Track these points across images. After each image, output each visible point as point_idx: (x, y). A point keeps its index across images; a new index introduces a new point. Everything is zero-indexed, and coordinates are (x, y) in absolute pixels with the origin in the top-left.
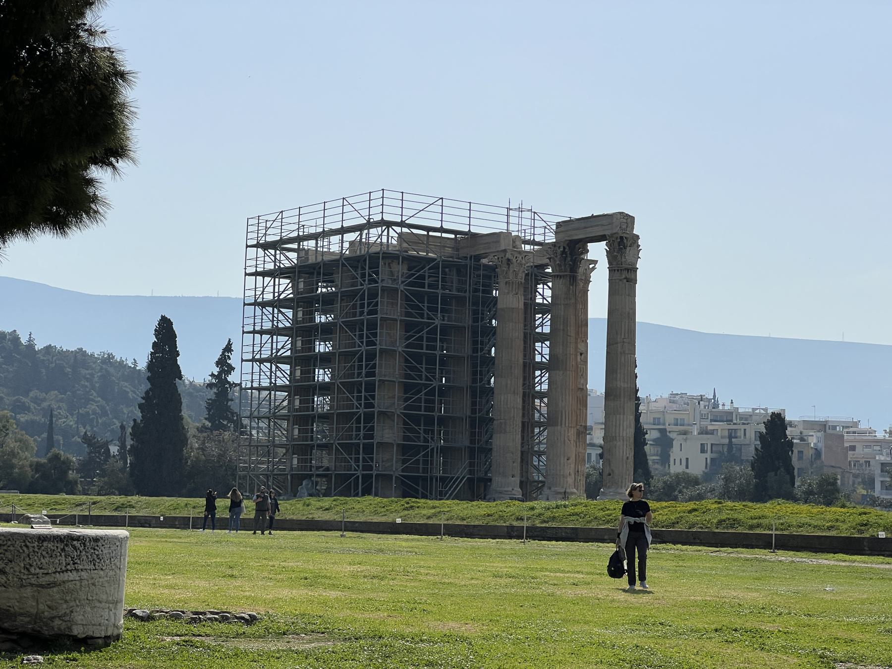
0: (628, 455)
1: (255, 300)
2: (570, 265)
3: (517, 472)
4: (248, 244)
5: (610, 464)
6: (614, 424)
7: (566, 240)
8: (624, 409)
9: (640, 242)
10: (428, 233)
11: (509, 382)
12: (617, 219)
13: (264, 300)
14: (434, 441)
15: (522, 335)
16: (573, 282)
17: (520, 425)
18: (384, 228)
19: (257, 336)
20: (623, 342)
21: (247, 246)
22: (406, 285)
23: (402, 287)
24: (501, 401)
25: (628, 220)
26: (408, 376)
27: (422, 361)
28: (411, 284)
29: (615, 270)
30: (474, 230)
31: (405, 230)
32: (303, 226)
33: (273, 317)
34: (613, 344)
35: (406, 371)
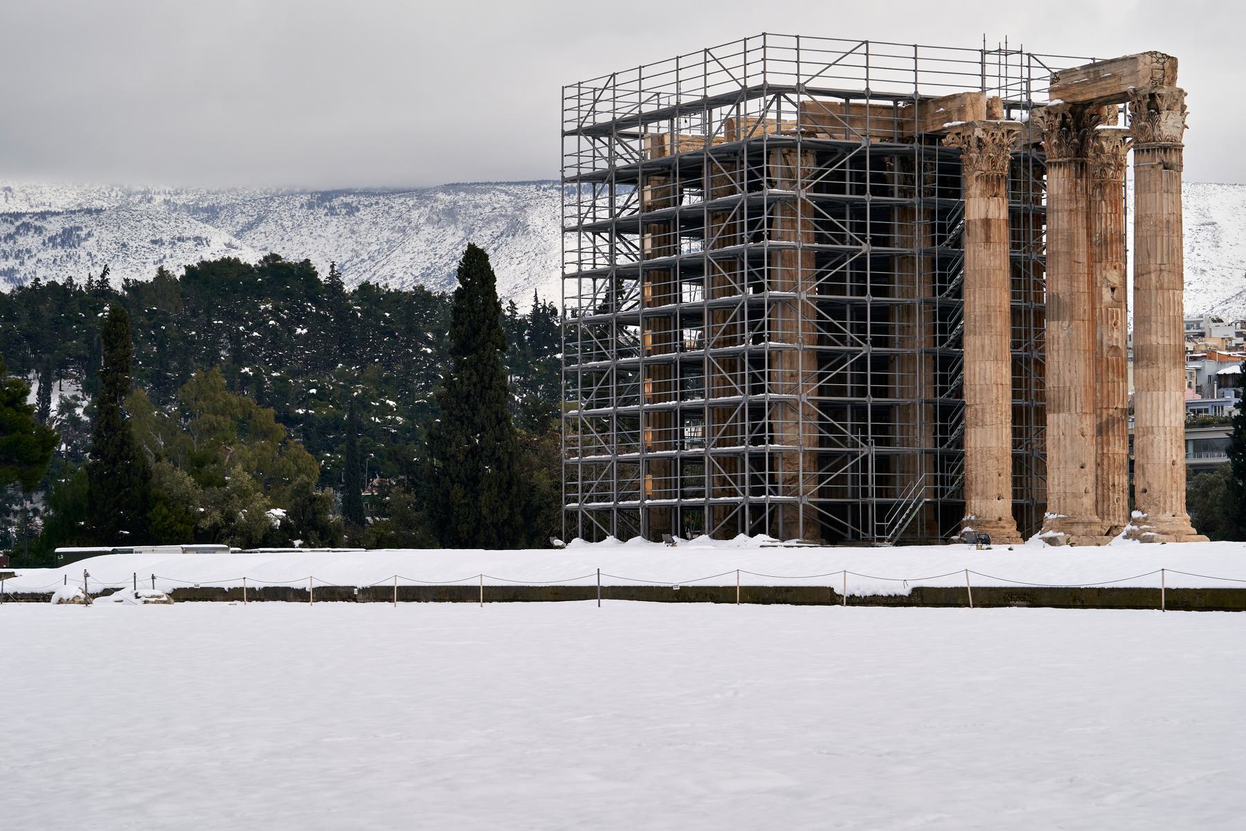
0: (1174, 458)
1: (580, 222)
2: (1075, 144)
3: (1007, 488)
4: (566, 130)
5: (1144, 474)
6: (1149, 406)
7: (1068, 103)
8: (1164, 382)
9: (1187, 101)
10: (847, 100)
11: (987, 342)
12: (1145, 64)
13: (597, 220)
14: (867, 444)
15: (1006, 265)
16: (1082, 173)
17: (1010, 413)
18: (770, 97)
19: (587, 282)
20: (1161, 270)
21: (564, 134)
22: (817, 188)
23: (803, 194)
24: (975, 375)
25: (1169, 65)
26: (821, 340)
27: (845, 311)
28: (817, 188)
29: (1143, 151)
30: (924, 91)
31: (805, 98)
32: (658, 94)
33: (611, 247)
34: (1143, 275)
35: (819, 331)
